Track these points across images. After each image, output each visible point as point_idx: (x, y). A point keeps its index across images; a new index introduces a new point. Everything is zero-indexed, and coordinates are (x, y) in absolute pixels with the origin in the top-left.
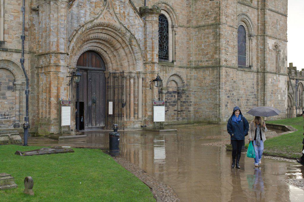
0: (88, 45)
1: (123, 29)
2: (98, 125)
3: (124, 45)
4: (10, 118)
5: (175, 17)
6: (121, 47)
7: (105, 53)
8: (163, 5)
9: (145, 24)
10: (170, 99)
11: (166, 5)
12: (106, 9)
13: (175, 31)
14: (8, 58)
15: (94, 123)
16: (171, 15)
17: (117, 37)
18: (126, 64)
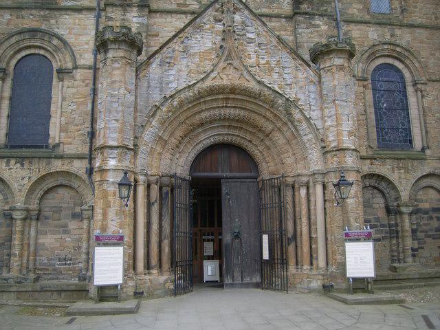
0: (210, 133)
1: (266, 92)
2: (247, 280)
3: (279, 124)
4: (74, 264)
5: (417, 65)
6: (276, 129)
7: (250, 145)
8: (386, 47)
9: (320, 77)
10: (426, 225)
11: (392, 47)
12: (226, 60)
13: (421, 92)
14: (65, 168)
15: (237, 274)
16: (408, 62)
17: (262, 111)
18: (290, 161)
